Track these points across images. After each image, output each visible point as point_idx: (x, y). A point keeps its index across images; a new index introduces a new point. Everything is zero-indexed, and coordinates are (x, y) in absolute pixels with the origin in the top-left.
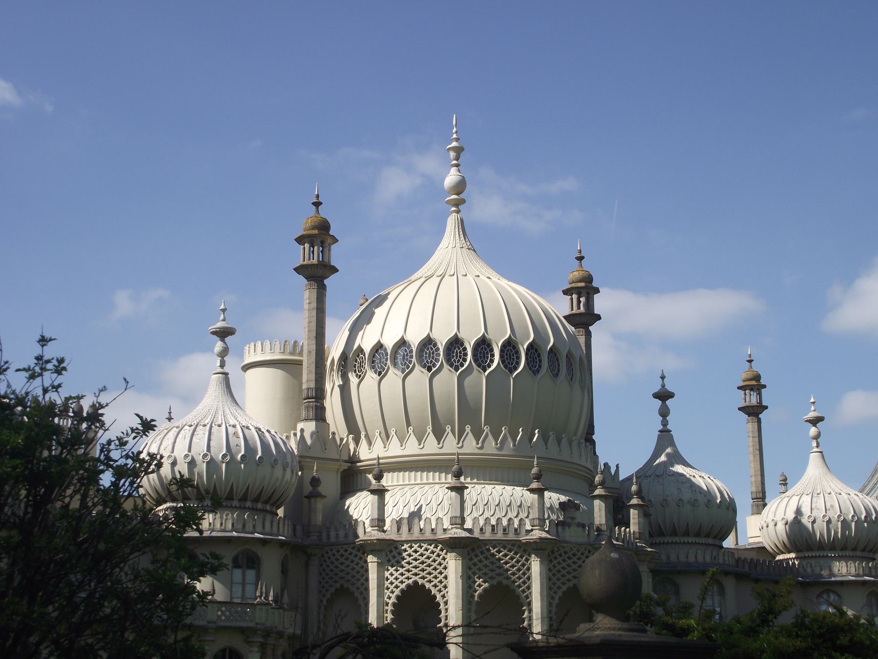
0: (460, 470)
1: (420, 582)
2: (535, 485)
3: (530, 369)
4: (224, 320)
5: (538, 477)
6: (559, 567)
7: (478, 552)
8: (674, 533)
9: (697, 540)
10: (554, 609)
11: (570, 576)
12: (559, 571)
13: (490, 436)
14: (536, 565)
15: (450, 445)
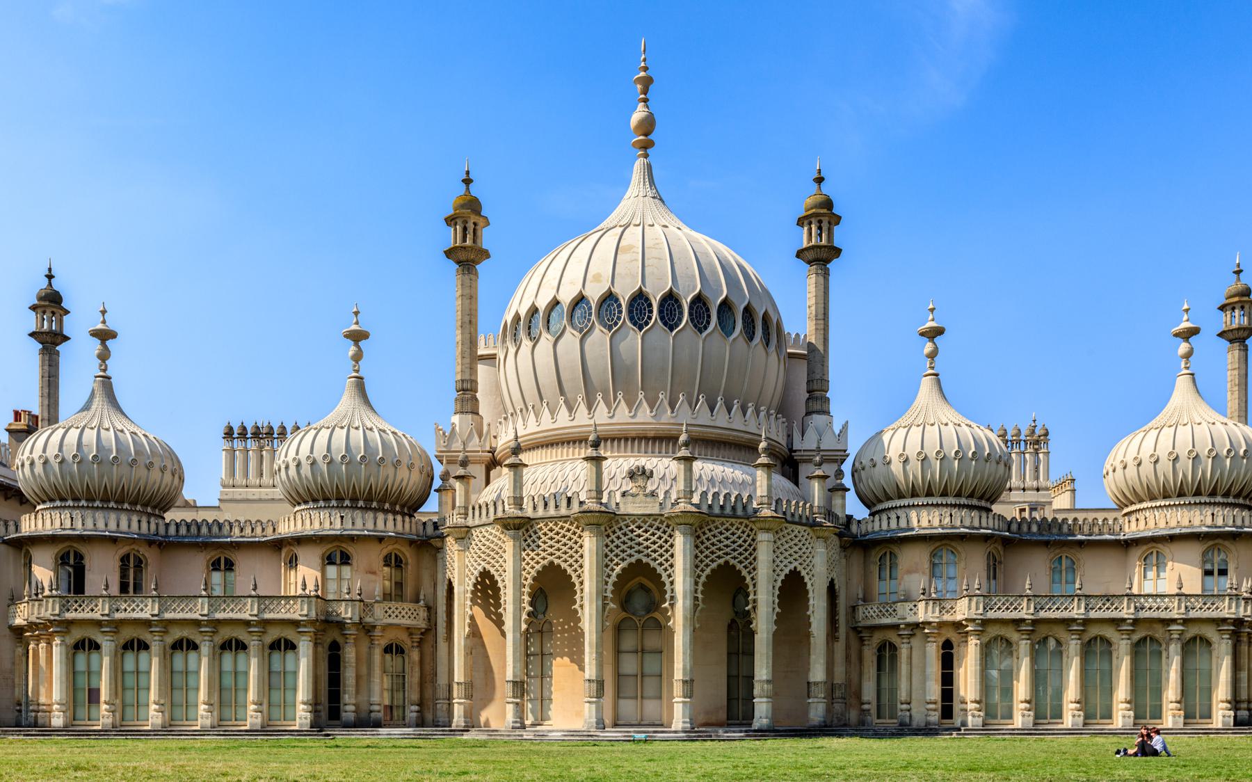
0: (596, 444)
1: (488, 567)
2: (684, 452)
3: (695, 326)
4: (357, 323)
5: (686, 444)
6: (617, 542)
7: (531, 532)
8: (901, 496)
9: (930, 500)
10: (610, 587)
11: (632, 552)
12: (617, 547)
13: (645, 404)
14: (679, 541)
15: (582, 420)
